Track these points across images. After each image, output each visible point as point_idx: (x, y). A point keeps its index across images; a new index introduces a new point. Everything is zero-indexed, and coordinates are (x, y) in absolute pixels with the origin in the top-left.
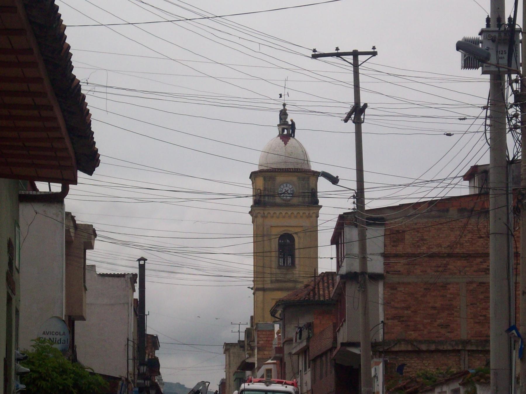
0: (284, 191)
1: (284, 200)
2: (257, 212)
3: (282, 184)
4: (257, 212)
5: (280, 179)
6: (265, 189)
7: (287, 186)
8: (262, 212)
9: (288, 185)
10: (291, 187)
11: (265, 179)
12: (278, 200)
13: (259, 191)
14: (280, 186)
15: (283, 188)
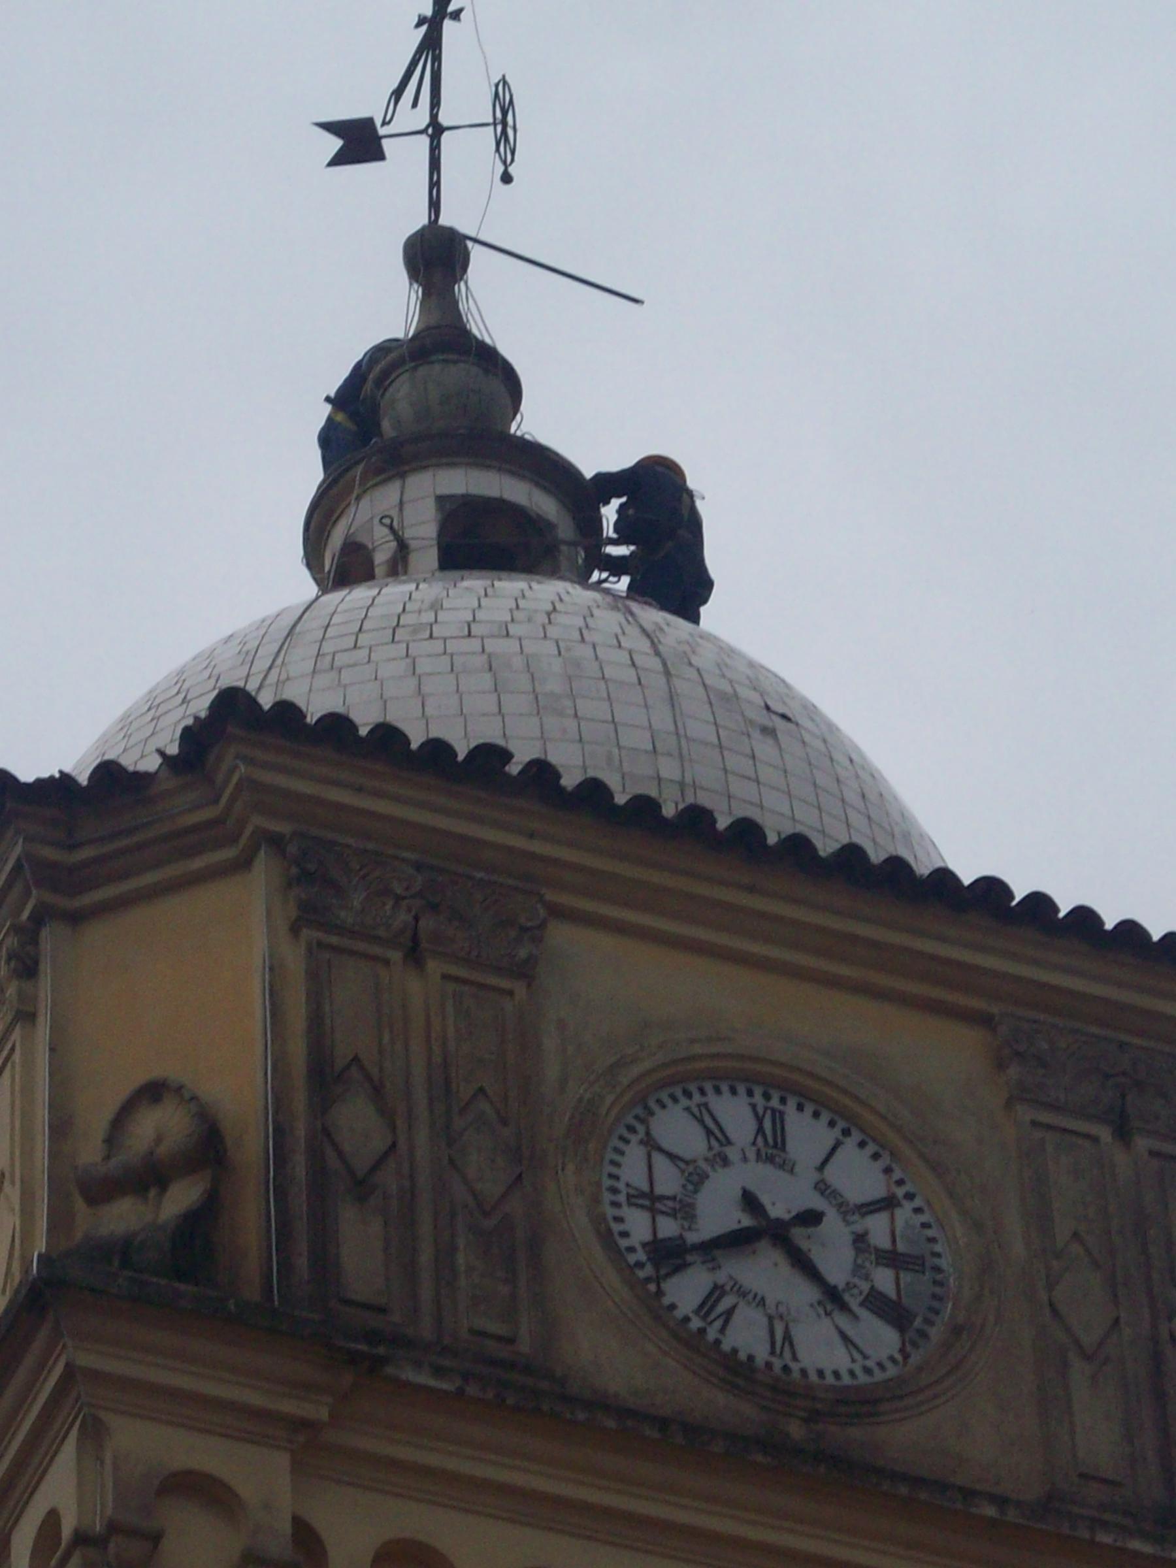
0: (718, 1213)
1: (736, 1371)
2: (149, 1443)
3: (692, 1076)
4: (149, 1443)
5: (613, 983)
6: (326, 1077)
7: (773, 1148)
8: (262, 1478)
9: (807, 1135)
10: (859, 1176)
11: (316, 880)
12: (605, 1352)
13: (161, 1128)
14: (643, 1104)
15: (705, 1163)
